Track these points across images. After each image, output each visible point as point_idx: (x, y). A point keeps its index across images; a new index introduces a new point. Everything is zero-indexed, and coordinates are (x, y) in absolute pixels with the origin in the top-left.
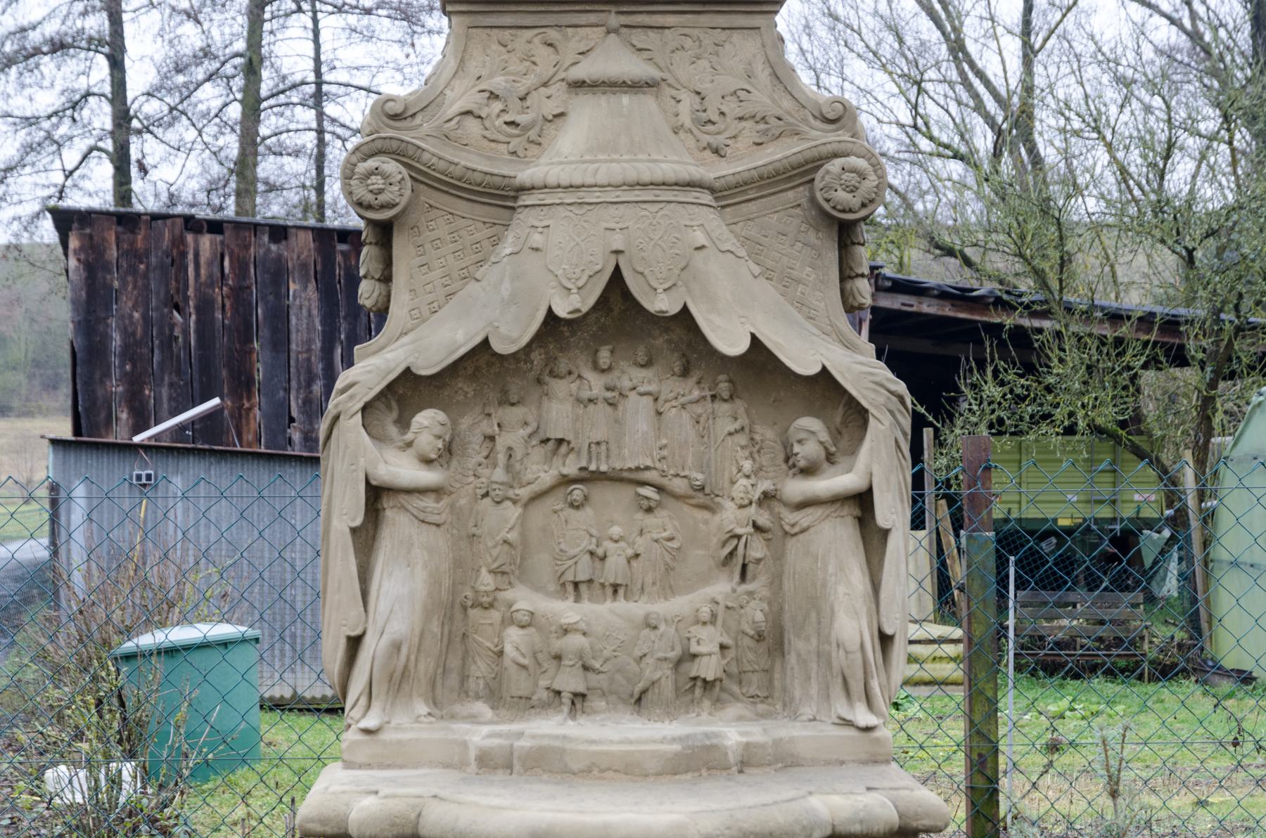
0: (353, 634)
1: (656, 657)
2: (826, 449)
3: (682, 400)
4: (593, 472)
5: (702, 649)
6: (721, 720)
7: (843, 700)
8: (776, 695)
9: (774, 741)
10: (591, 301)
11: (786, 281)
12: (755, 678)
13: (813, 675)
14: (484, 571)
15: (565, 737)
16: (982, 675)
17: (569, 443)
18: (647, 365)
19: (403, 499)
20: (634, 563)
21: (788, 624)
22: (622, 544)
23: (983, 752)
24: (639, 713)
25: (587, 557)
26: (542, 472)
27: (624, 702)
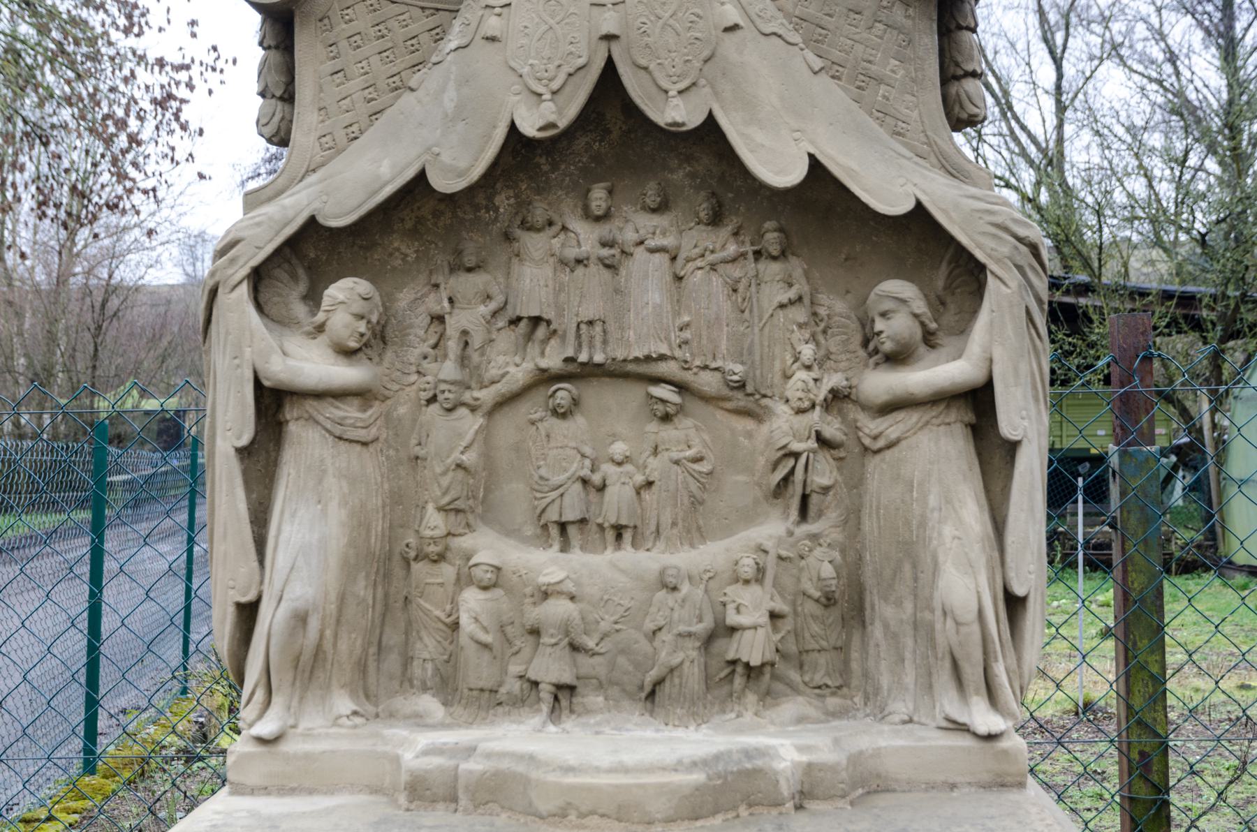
0: (243, 600)
1: (675, 631)
2: (923, 324)
3: (710, 258)
4: (583, 364)
5: (743, 620)
6: (772, 723)
7: (953, 693)
8: (855, 682)
9: (849, 759)
10: (572, 111)
11: (861, 81)
12: (822, 659)
13: (908, 655)
14: (430, 508)
15: (531, 759)
16: (1143, 644)
17: (549, 322)
18: (661, 208)
19: (310, 406)
20: (646, 495)
21: (869, 579)
22: (628, 467)
23: (1147, 749)
24: (652, 713)
25: (578, 486)
26: (511, 365)
27: (631, 696)
